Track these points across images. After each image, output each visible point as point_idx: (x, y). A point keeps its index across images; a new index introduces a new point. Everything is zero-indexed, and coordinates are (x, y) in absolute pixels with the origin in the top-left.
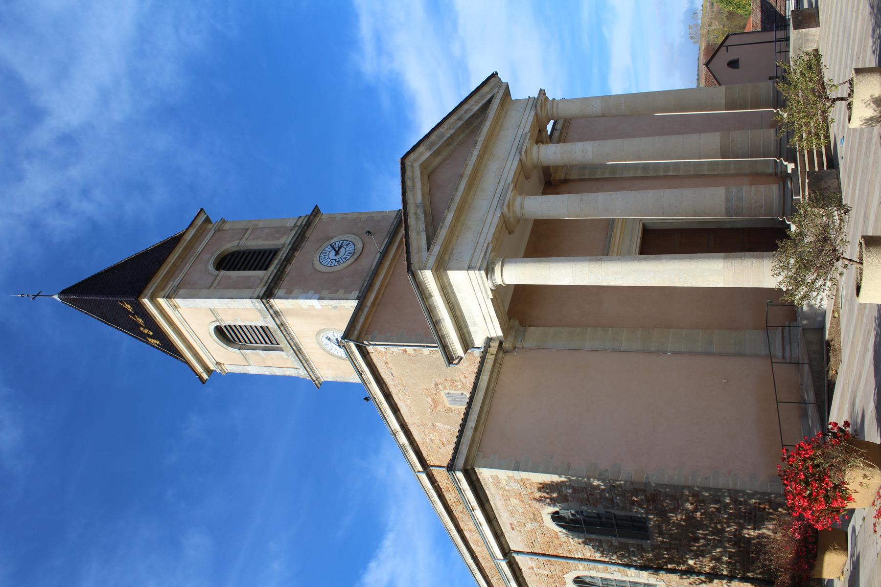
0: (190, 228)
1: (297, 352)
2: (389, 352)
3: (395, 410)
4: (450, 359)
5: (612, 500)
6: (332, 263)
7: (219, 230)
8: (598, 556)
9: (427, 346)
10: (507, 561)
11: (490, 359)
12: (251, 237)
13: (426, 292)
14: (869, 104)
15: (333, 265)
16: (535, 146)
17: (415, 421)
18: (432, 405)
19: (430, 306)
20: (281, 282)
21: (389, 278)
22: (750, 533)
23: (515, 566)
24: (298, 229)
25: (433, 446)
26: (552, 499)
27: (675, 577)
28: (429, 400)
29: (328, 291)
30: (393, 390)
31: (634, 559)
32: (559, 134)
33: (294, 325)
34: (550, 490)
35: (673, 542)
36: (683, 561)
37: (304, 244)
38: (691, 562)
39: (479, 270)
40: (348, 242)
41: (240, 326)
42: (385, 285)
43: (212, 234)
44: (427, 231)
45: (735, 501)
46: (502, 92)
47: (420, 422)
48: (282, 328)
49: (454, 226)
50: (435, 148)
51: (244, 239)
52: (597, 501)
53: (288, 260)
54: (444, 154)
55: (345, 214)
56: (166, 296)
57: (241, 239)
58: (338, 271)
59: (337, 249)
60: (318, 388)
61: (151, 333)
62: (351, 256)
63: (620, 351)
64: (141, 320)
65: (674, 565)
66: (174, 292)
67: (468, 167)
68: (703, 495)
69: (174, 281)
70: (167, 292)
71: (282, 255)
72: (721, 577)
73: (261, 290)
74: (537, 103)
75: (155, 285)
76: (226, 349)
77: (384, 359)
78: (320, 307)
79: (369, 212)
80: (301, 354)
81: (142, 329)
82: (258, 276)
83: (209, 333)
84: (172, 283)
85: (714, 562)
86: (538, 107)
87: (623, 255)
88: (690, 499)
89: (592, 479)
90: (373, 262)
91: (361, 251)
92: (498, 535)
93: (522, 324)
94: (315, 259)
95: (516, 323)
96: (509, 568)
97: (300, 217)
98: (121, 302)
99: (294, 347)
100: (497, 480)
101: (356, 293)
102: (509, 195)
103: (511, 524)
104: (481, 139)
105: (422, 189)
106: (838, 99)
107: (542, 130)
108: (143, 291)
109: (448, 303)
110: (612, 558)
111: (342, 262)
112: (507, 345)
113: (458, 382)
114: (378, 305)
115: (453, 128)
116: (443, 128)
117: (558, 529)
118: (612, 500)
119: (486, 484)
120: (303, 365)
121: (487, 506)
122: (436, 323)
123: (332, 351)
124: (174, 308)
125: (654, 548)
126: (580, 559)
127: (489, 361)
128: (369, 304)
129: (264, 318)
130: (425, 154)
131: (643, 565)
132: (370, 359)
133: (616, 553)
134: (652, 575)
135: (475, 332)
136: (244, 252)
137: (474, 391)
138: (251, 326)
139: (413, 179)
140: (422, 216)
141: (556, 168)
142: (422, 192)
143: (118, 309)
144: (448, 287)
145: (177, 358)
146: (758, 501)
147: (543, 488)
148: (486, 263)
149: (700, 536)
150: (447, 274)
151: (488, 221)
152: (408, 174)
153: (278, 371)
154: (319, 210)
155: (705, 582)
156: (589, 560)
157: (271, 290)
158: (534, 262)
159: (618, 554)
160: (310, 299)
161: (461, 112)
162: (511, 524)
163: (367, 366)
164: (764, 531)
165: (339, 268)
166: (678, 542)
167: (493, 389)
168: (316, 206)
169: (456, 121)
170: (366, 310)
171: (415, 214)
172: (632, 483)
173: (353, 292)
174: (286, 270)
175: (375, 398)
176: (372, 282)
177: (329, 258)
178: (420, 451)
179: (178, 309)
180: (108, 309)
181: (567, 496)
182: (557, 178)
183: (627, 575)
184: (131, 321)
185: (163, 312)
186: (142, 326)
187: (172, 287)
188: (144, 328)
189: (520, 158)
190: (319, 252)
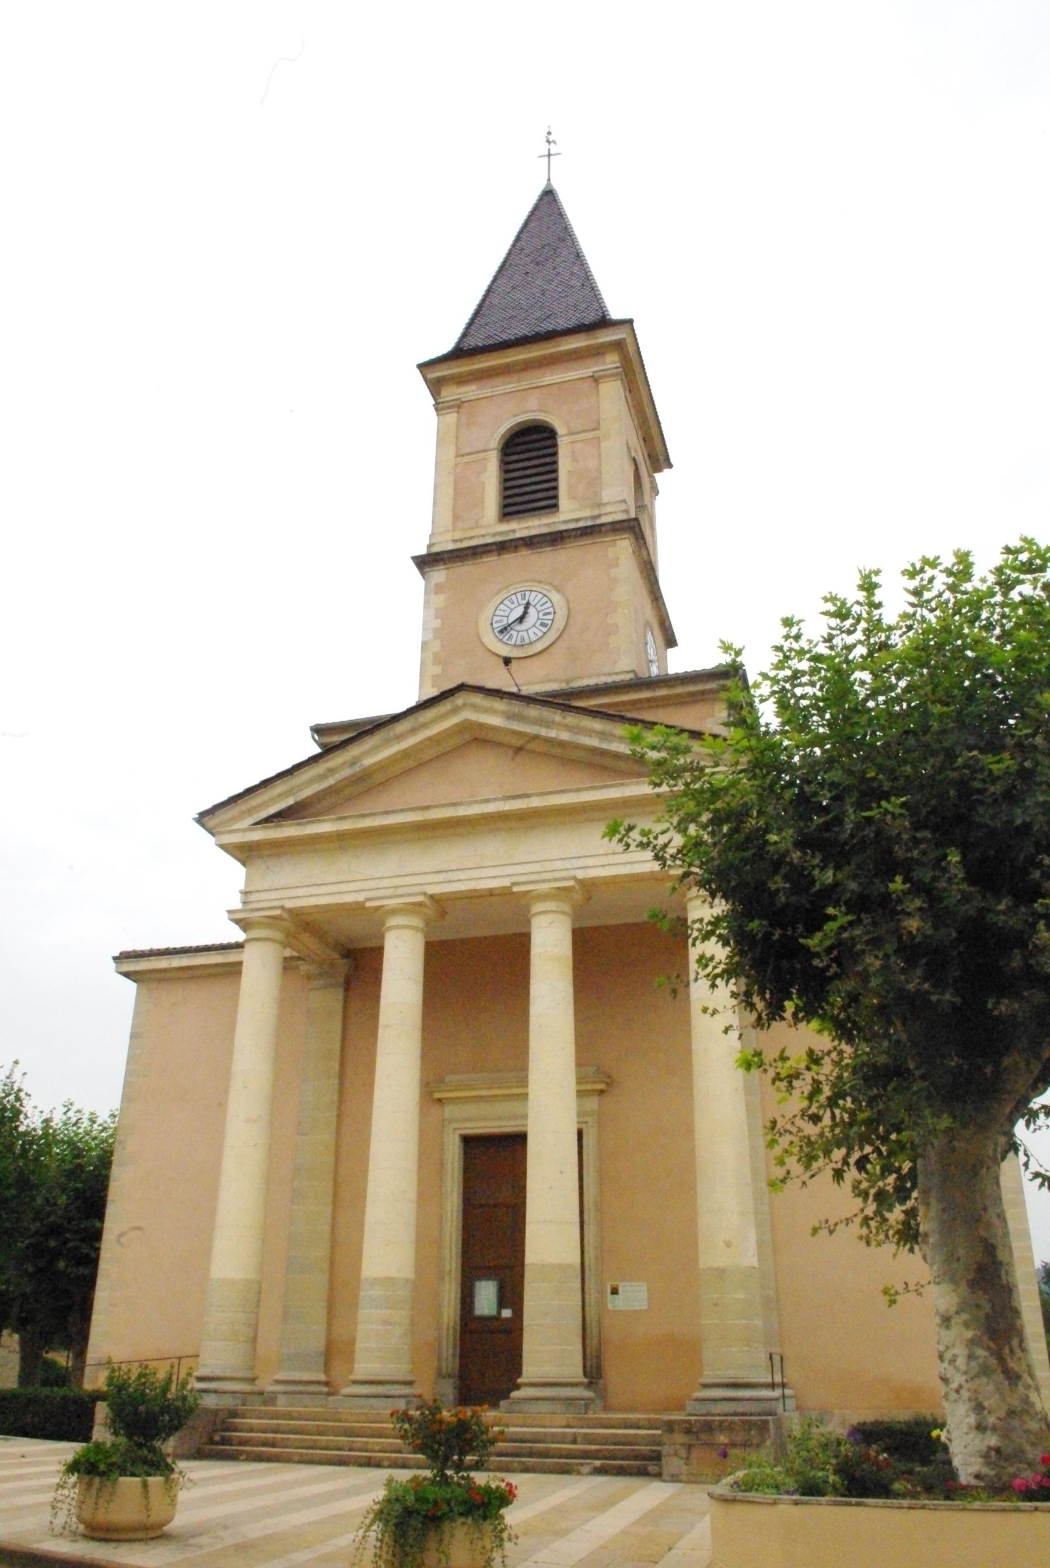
43: (575, 377)
116: (564, 718)
151: (344, 887)
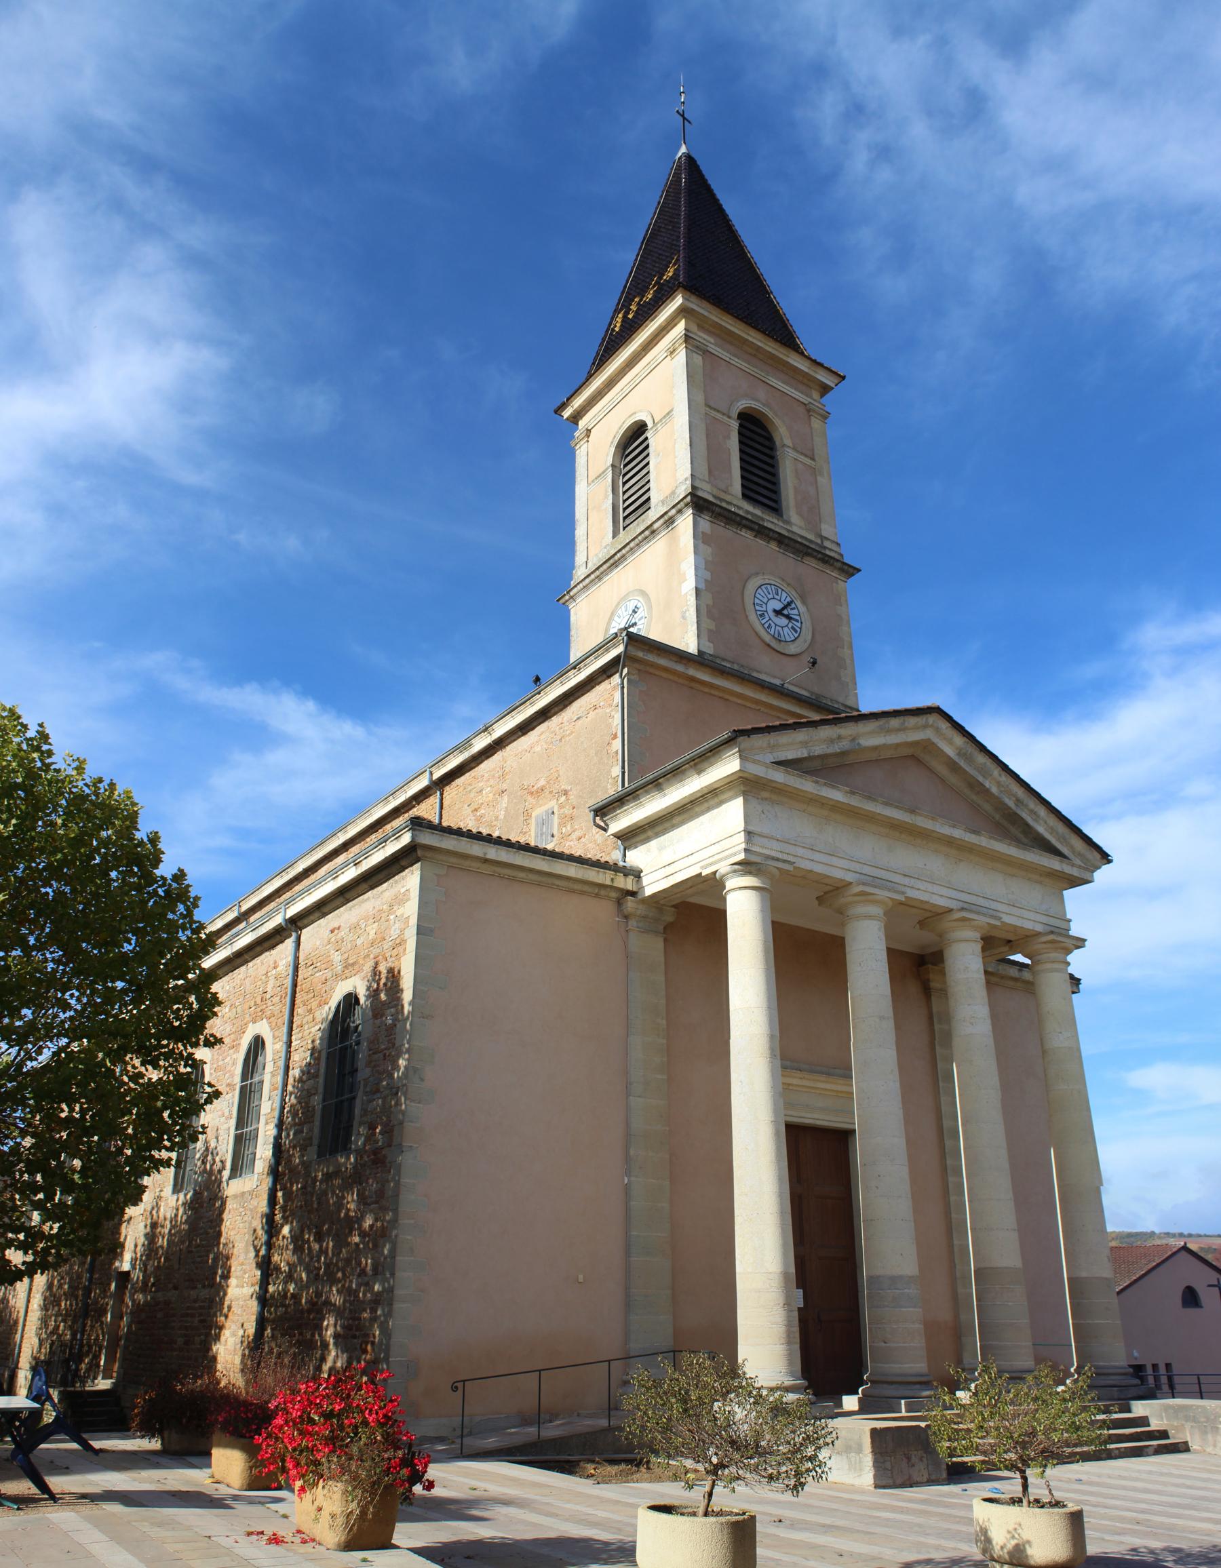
0: (809, 361)
1: (611, 561)
2: (612, 711)
3: (524, 728)
4: (603, 811)
5: (378, 1091)
6: (761, 605)
7: (809, 411)
8: (295, 1073)
9: (623, 773)
10: (283, 924)
11: (604, 877)
12: (800, 466)
13: (705, 764)
14: (1013, 1537)
15: (757, 608)
16: (978, 935)
17: (508, 762)
18: (535, 788)
19: (683, 772)
20: (722, 524)
21: (739, 701)
22: (330, 1327)
23: (278, 938)
24: (817, 544)
25: (472, 794)
26: (377, 991)
27: (262, 1205)
28: (542, 782)
29: (710, 603)
30: (555, 721)
31: (291, 1133)
32: (1013, 975)
33: (656, 549)
34: (390, 988)
35: (314, 1199)
36: (288, 1217)
37: (792, 555)
38: (286, 1230)
39: (746, 850)
40: (799, 630)
41: (648, 463)
42: (727, 697)
43: (801, 399)
44: (810, 758)
45: (377, 1300)
46: (1075, 872)
47: (507, 770)
48: (647, 533)
49: (823, 804)
50: (962, 764)
51: (794, 454)
52: (375, 1066)
53: (762, 532)
54: (953, 779)
55: (848, 622)
56: (689, 334)
57: (795, 449)
58: (747, 617)
59: (785, 612)
60: (558, 601)
61: (630, 316)
62: (774, 636)
63: (628, 1095)
64: (650, 296)
65: (281, 1201)
66: (697, 347)
67: (931, 821)
68: (385, 1246)
69: (716, 345)
70: (696, 334)
71: (770, 521)
72: (264, 1282)
73: (706, 493)
74: (1059, 934)
75: (706, 314)
76: (612, 442)
77: (602, 704)
78: (683, 593)
79: (853, 661)
80: (610, 567)
81: (637, 300)
82: (731, 486)
83: (635, 413)
84: (712, 341)
85: (287, 1269)
86: (1051, 937)
87: (784, 1094)
88: (379, 1224)
89: (407, 1056)
90: (765, 673)
91: (783, 652)
92: (321, 908)
93: (668, 928)
94: (765, 577)
95: (669, 917)
96: (274, 929)
97: (838, 544)
98: (677, 260)
99: (619, 555)
100: (401, 900)
101: (709, 649)
102: (883, 894)
103: (339, 928)
104: (983, 841)
105: (884, 746)
106: (1025, 1479)
107: (1012, 944)
108: (694, 293)
109: (691, 802)
110: (293, 1096)
111: (763, 622)
112: (630, 903)
113: (572, 827)
114: (691, 688)
115: (1001, 791)
116: (1000, 775)
117: (333, 1004)
118: (378, 1091)
119: (396, 882)
120: (592, 573)
121: (364, 886)
122: (656, 784)
123: (616, 618)
124: (671, 350)
125: (306, 1165)
126: (289, 1043)
127: (601, 874)
128: (692, 672)
129: (663, 502)
130: (950, 746)
131: (283, 1148)
132: (599, 680)
133: (299, 1102)
134: (267, 1165)
135: (649, 851)
136: (772, 457)
137: (548, 853)
138: (649, 481)
139: (902, 729)
140: (836, 748)
141: (943, 973)
142: (880, 746)
143: (667, 257)
144: (716, 800)
145: (594, 364)
146: (377, 1340)
147: (393, 976)
148: (759, 861)
149: (325, 1244)
150: (736, 797)
151: (835, 861)
152: (912, 721)
153: (581, 533)
154: (853, 575)
155: (257, 1256)
156: (288, 1058)
157: (708, 509)
158: (765, 942)
159: (298, 1106)
160: (696, 575)
161: (1032, 803)
162: (339, 928)
163: (588, 677)
164: (333, 1353)
165: (753, 617)
166: (315, 1206)
167: (554, 885)
168: (859, 570)
169: (1014, 795)
170: (680, 668)
171: (840, 737)
172: (401, 1123)
173: (711, 645)
174: (744, 530)
175: (539, 693)
176: (728, 673)
177: (769, 600)
178: (463, 774)
179: (669, 357)
180: (665, 239)
181: (382, 1017)
182: (931, 976)
183: (267, 1123)
184: (648, 280)
185: (664, 332)
186: (641, 300)
187: (704, 342)
188: (639, 304)
189: (952, 910)
190: (778, 582)
